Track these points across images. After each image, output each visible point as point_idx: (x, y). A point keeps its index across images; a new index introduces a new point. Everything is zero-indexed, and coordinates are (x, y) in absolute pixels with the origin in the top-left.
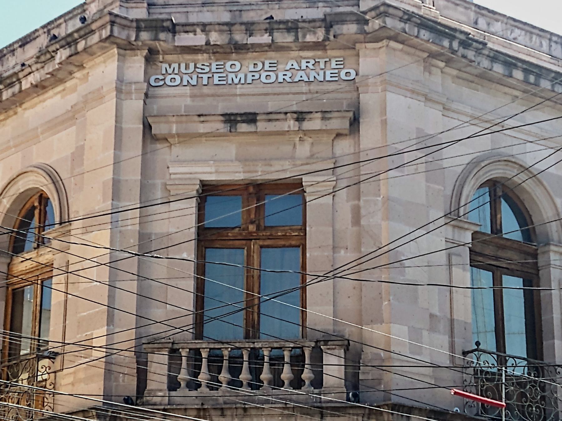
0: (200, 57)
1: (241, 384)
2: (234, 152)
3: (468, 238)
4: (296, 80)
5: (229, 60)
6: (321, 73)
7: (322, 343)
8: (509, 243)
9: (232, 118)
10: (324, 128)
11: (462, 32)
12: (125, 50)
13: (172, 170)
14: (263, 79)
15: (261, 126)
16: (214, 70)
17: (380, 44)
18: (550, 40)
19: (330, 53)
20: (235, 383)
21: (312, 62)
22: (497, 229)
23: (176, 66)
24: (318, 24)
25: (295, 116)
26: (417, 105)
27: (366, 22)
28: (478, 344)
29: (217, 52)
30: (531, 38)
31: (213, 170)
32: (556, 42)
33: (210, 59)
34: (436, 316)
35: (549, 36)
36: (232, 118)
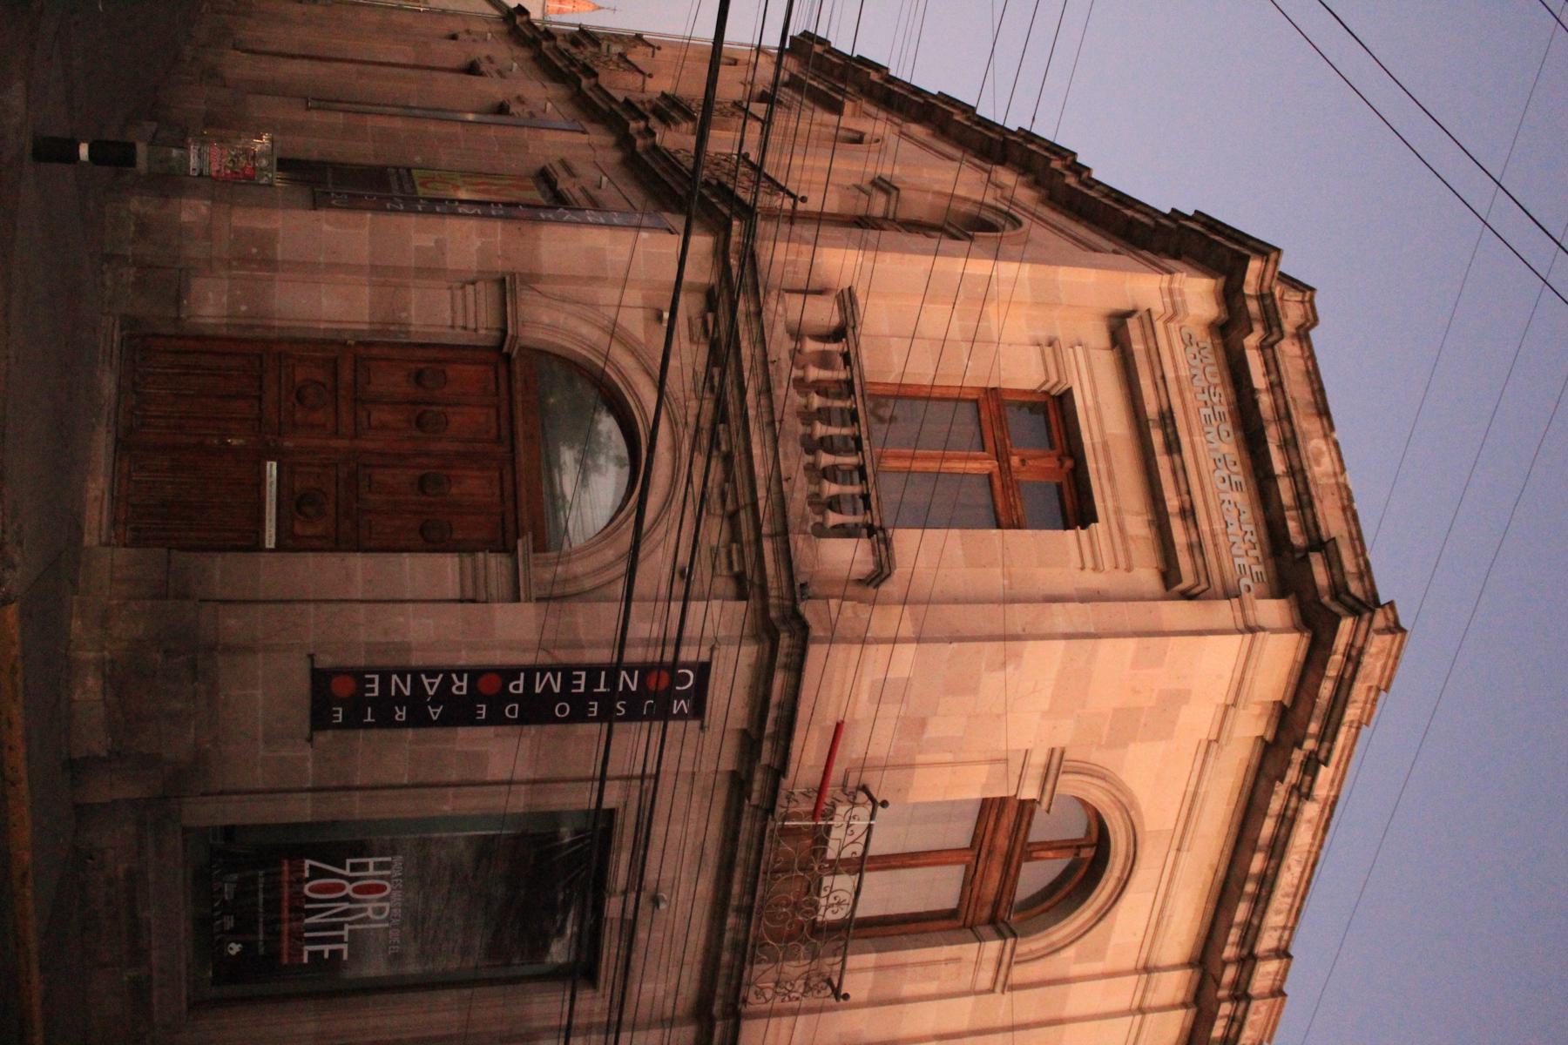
2: (1114, 431)
3: (1029, 792)
8: (1012, 872)
9: (1168, 421)
11: (1330, 751)
13: (1079, 349)
16: (1217, 409)
18: (1284, 928)
20: (808, 416)
22: (1031, 852)
25: (1187, 506)
26: (1221, 692)
28: (884, 804)
30: (1287, 895)
32: (1280, 939)
34: (923, 733)
36: (1168, 421)
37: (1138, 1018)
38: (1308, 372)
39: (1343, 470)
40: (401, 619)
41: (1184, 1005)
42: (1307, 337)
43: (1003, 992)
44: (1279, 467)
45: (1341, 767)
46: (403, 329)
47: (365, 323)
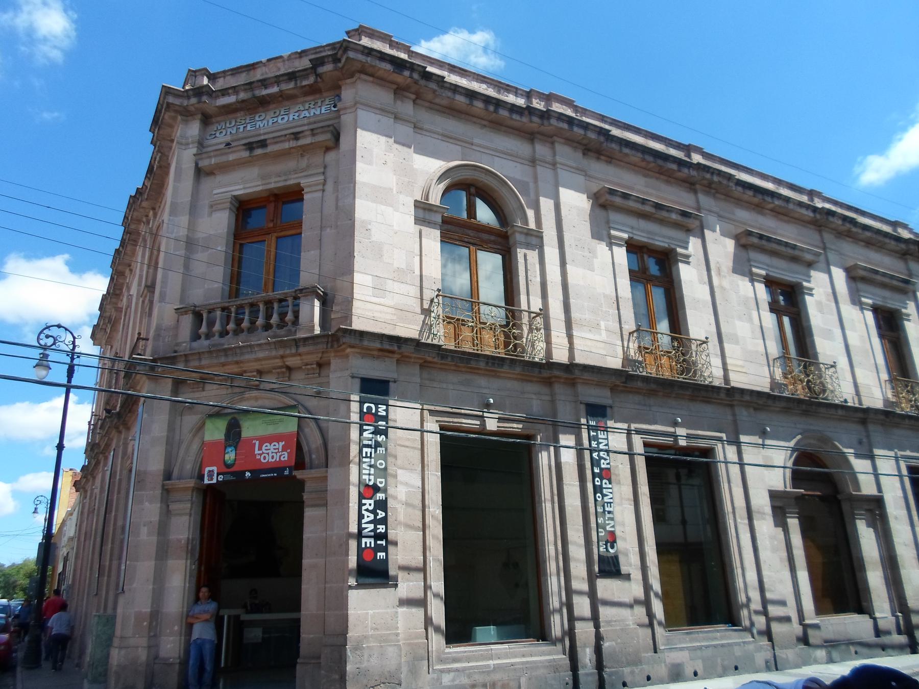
0: (239, 114)
1: (242, 331)
4: (301, 117)
5: (258, 113)
6: (319, 110)
7: (298, 292)
10: (313, 141)
12: (187, 116)
14: (280, 121)
15: (270, 149)
16: (248, 121)
17: (354, 79)
19: (325, 94)
21: (313, 103)
23: (223, 124)
24: (309, 71)
27: (339, 60)
29: (250, 109)
31: (241, 187)
33: (246, 115)
35: (515, 90)
37: (558, 165)
38: (232, 74)
39: (281, 57)
40: (334, 538)
41: (553, 143)
42: (214, 74)
43: (542, 232)
44: (275, 89)
45: (433, 61)
46: (190, 542)
47: (186, 562)
